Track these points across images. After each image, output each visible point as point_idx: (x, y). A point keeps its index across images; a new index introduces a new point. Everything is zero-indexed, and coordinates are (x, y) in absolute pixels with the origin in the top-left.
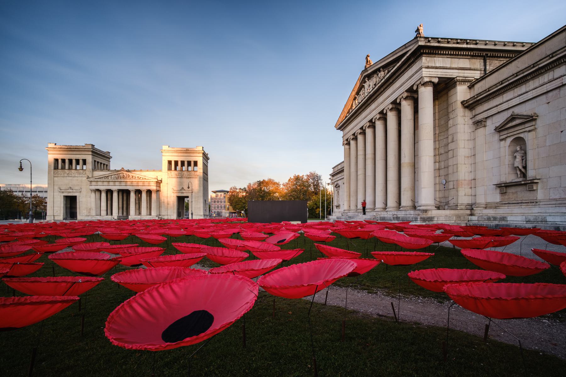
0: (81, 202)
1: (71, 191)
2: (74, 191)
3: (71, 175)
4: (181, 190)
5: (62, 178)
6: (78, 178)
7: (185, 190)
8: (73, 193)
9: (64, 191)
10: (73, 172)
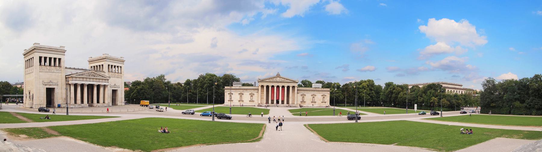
0: (58, 93)
1: (52, 84)
2: (54, 84)
5: (45, 73)
7: (116, 86)
9: (47, 84)
10: (53, 69)
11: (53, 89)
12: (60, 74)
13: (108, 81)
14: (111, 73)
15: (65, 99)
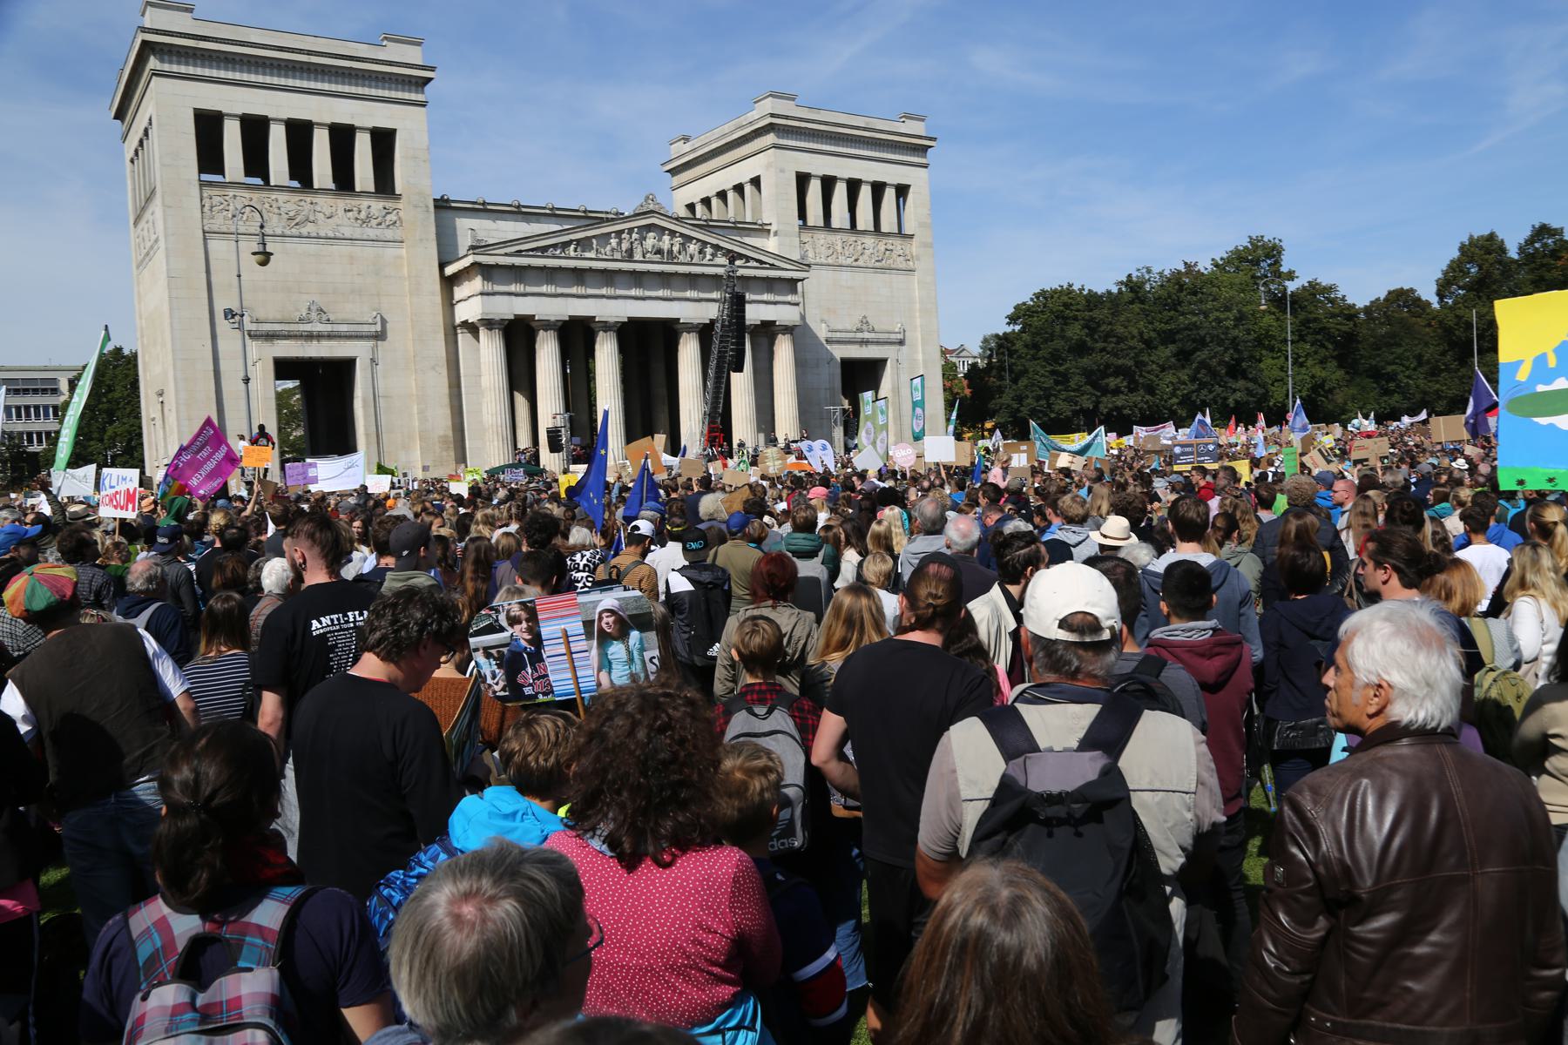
2: (344, 328)
3: (308, 229)
4: (859, 330)
6: (357, 250)
7: (873, 330)
8: (333, 343)
9: (277, 327)
11: (345, 368)
12: (390, 252)
13: (794, 291)
14: (822, 238)
15: (443, 440)
